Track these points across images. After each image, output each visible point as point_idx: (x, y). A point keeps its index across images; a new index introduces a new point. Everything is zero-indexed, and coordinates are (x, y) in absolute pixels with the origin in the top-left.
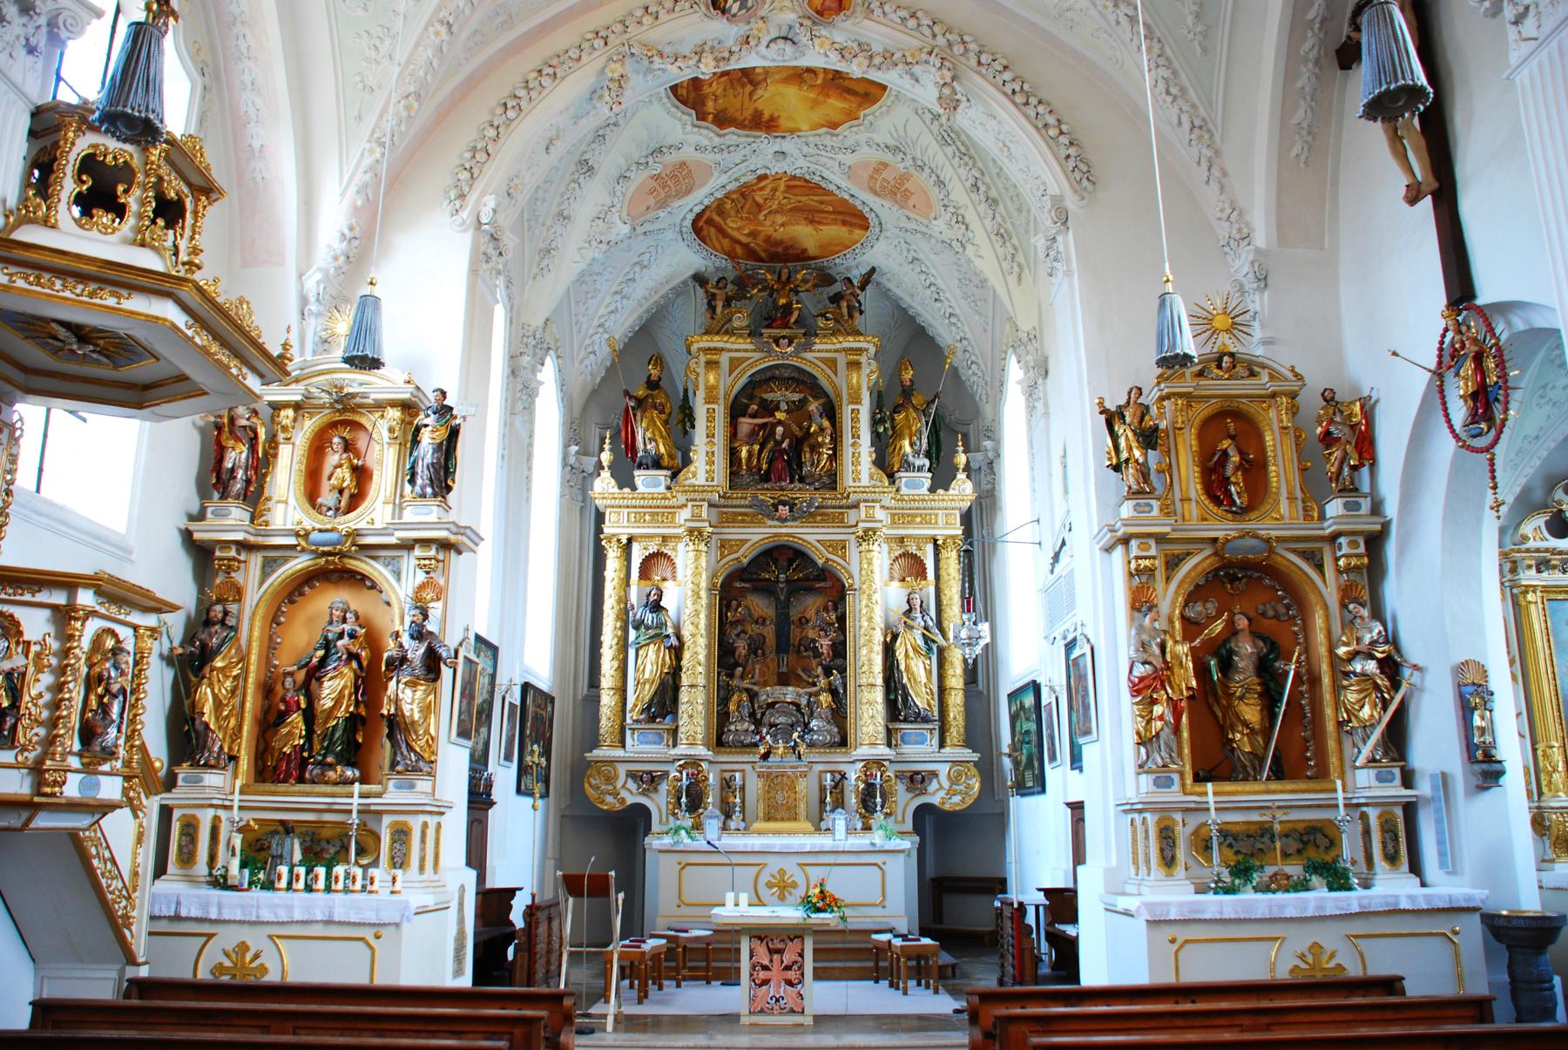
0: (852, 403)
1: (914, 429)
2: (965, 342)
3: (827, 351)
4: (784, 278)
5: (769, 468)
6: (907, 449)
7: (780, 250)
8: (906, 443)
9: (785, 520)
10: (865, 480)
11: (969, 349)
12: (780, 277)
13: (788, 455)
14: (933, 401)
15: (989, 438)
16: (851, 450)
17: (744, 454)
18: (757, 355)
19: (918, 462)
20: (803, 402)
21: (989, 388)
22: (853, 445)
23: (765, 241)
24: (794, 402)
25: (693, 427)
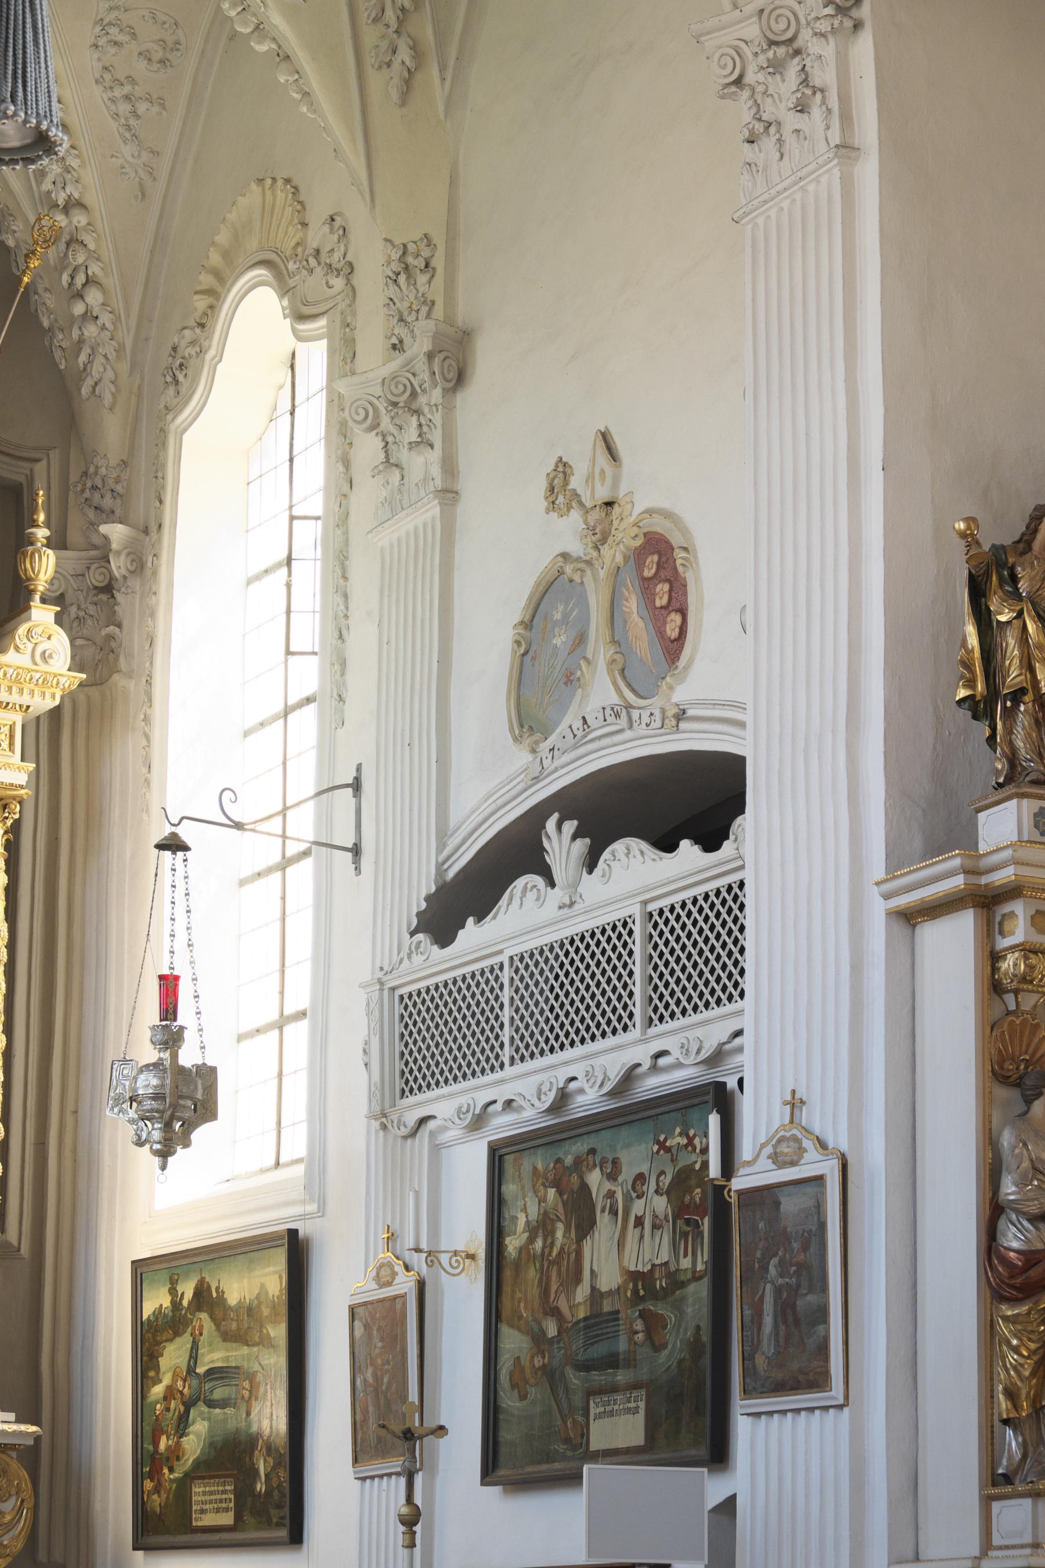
2: (79, 219)
11: (88, 239)
15: (111, 516)
21: (124, 367)
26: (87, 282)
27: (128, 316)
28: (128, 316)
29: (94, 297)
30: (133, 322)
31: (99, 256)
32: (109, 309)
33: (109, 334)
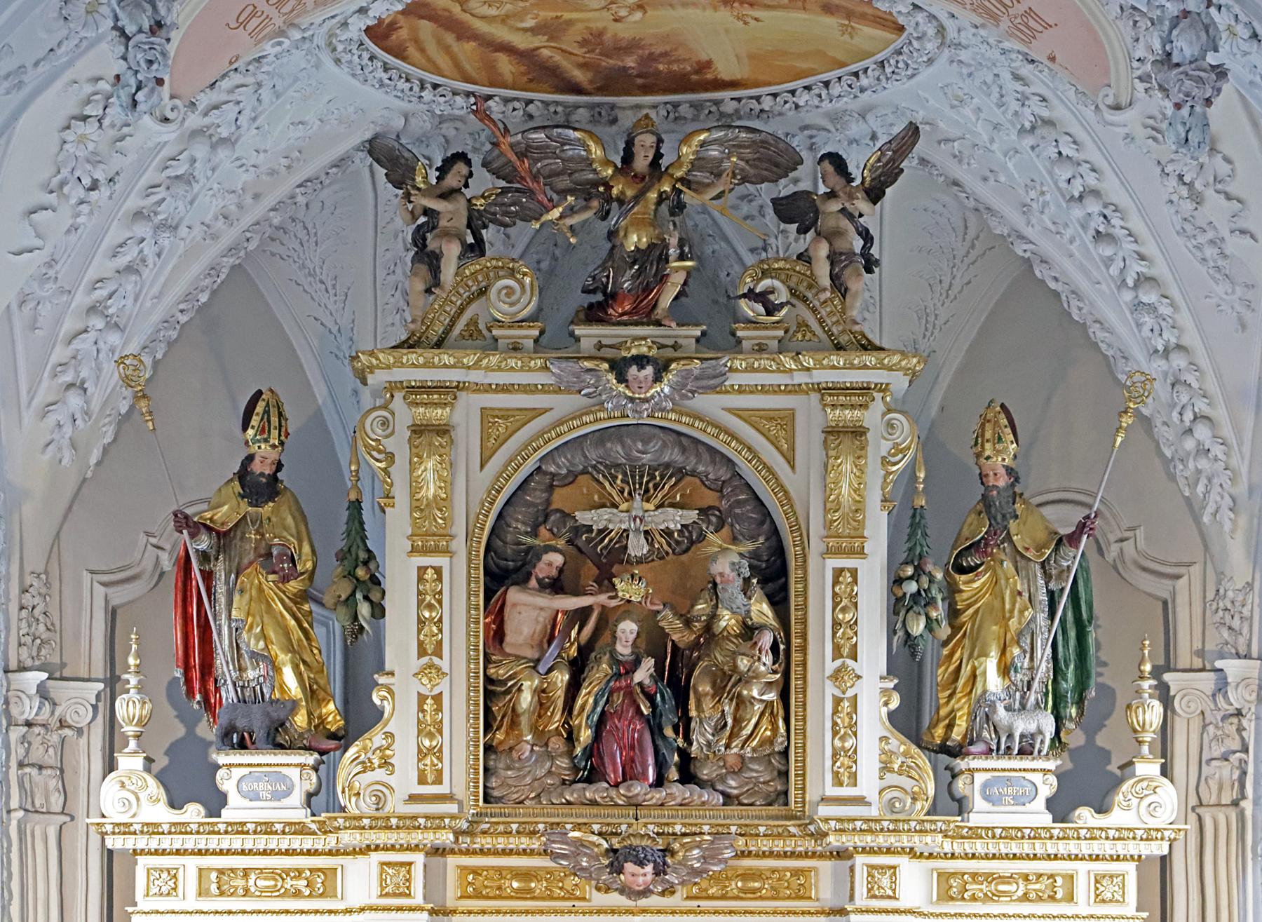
0: (839, 552)
1: (1013, 623)
3: (763, 390)
4: (641, 163)
5: (597, 737)
6: (993, 682)
7: (630, 62)
8: (991, 665)
9: (646, 893)
10: (868, 782)
12: (628, 157)
13: (651, 698)
14: (1073, 539)
16: (831, 690)
17: (526, 700)
18: (564, 404)
19: (1022, 725)
20: (690, 539)
22: (837, 676)
23: (584, 43)
24: (668, 533)
25: (379, 611)
26: (1195, 418)
27: (1240, 444)
28: (1240, 444)
29: (1202, 432)
30: (1247, 449)
31: (1205, 392)
32: (1220, 441)
33: (1223, 464)
